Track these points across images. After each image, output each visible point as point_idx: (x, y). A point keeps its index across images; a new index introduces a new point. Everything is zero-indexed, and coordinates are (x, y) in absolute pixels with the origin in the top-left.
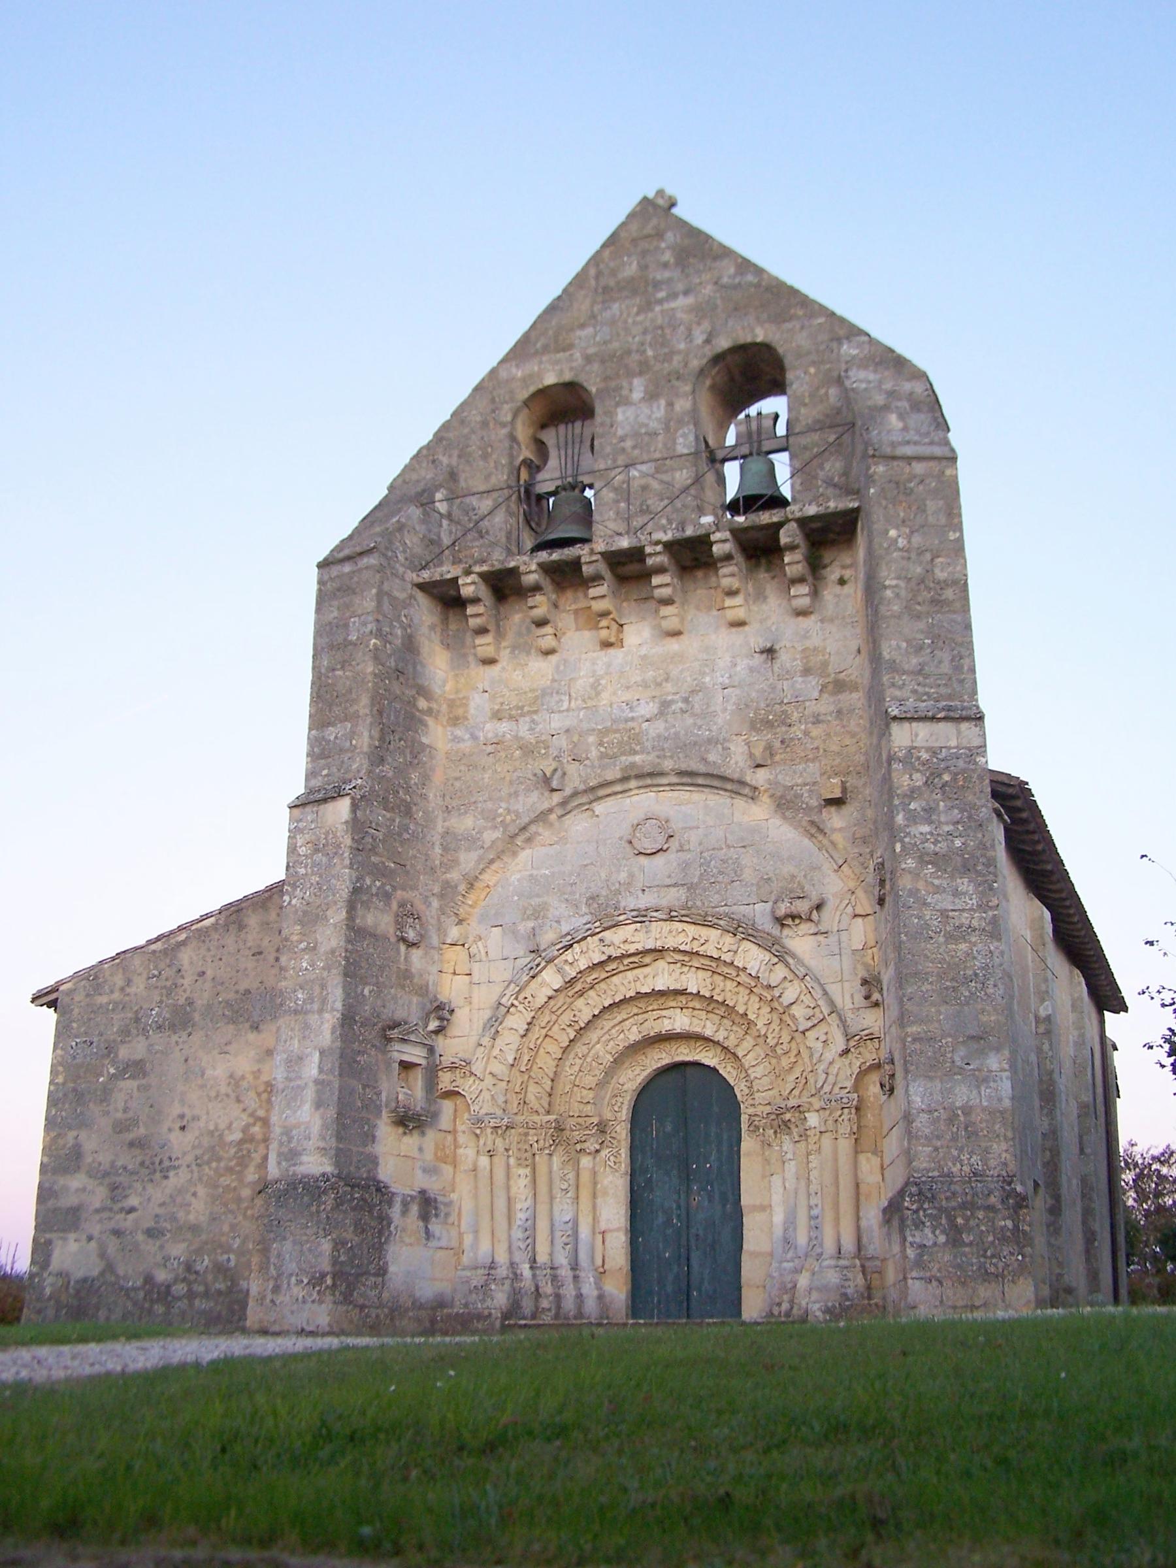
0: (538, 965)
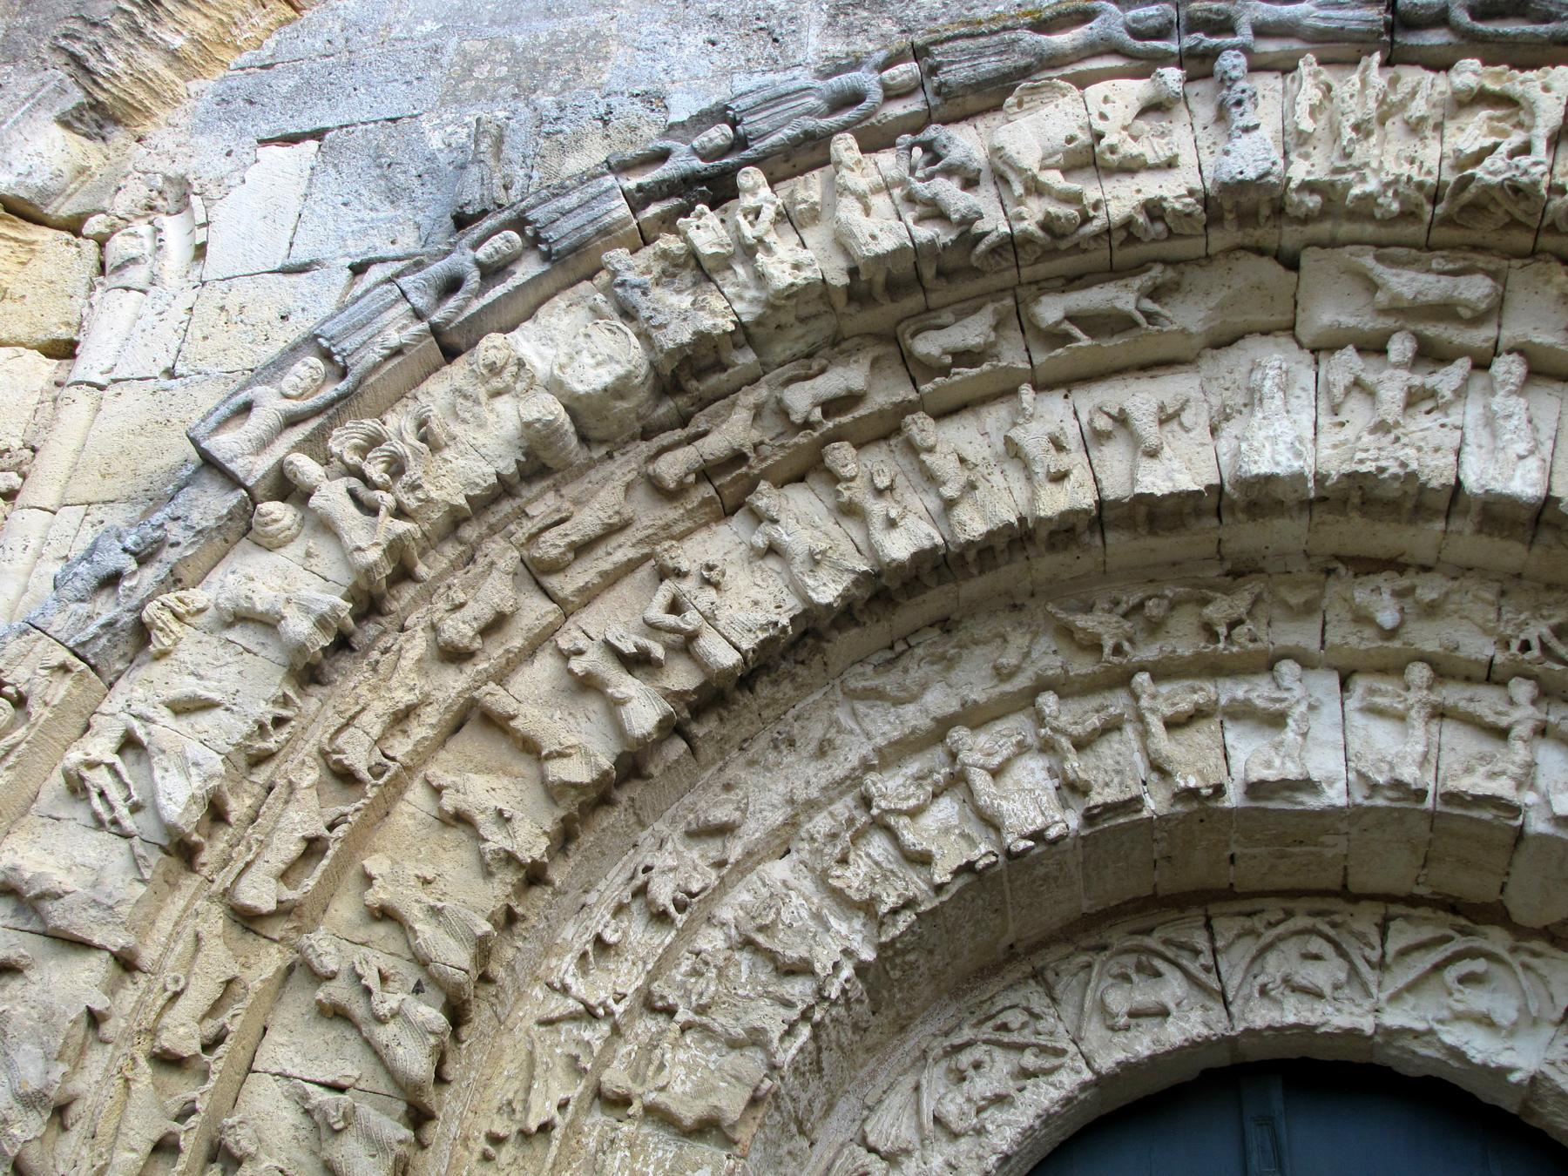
0: (492, 272)
